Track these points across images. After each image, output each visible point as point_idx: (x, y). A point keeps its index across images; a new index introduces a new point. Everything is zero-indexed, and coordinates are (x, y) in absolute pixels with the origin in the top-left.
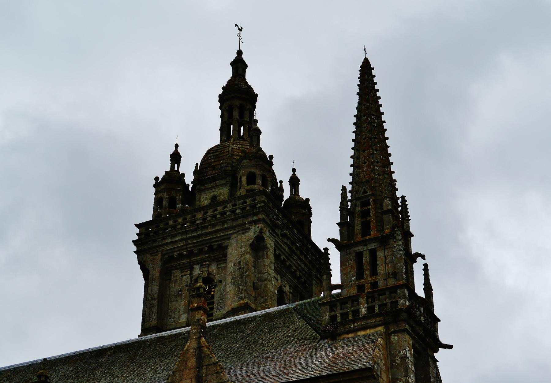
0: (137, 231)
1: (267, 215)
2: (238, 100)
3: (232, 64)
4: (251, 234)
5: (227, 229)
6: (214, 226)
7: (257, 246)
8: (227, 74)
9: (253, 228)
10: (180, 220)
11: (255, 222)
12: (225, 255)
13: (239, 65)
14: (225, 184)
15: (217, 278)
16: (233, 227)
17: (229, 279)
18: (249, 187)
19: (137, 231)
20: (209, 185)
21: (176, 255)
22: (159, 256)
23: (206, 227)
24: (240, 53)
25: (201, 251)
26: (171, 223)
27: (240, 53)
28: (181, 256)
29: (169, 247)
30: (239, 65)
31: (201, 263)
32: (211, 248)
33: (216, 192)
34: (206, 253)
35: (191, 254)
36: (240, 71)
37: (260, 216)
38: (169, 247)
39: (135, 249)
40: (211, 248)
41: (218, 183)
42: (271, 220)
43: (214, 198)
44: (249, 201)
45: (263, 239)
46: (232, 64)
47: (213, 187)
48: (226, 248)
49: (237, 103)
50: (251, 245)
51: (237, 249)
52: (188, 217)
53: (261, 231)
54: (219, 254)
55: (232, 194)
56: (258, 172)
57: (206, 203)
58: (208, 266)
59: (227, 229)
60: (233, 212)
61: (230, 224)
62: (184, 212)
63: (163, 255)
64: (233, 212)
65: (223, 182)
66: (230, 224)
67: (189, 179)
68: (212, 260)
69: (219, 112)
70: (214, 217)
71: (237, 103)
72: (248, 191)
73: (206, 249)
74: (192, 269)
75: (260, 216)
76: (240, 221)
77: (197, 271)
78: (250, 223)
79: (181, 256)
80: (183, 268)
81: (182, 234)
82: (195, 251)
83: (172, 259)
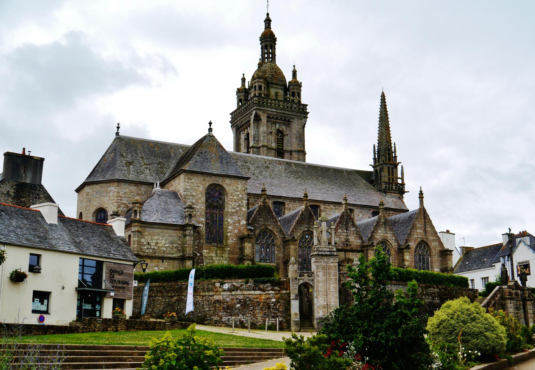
2: (268, 41)
13: (268, 21)
14: (282, 89)
20: (274, 86)
21: (271, 116)
22: (266, 115)
25: (281, 119)
28: (273, 118)
30: (268, 21)
31: (279, 123)
35: (277, 118)
40: (285, 119)
41: (278, 87)
48: (291, 122)
65: (280, 87)
68: (284, 124)
77: (277, 126)
79: (273, 118)
81: (277, 109)
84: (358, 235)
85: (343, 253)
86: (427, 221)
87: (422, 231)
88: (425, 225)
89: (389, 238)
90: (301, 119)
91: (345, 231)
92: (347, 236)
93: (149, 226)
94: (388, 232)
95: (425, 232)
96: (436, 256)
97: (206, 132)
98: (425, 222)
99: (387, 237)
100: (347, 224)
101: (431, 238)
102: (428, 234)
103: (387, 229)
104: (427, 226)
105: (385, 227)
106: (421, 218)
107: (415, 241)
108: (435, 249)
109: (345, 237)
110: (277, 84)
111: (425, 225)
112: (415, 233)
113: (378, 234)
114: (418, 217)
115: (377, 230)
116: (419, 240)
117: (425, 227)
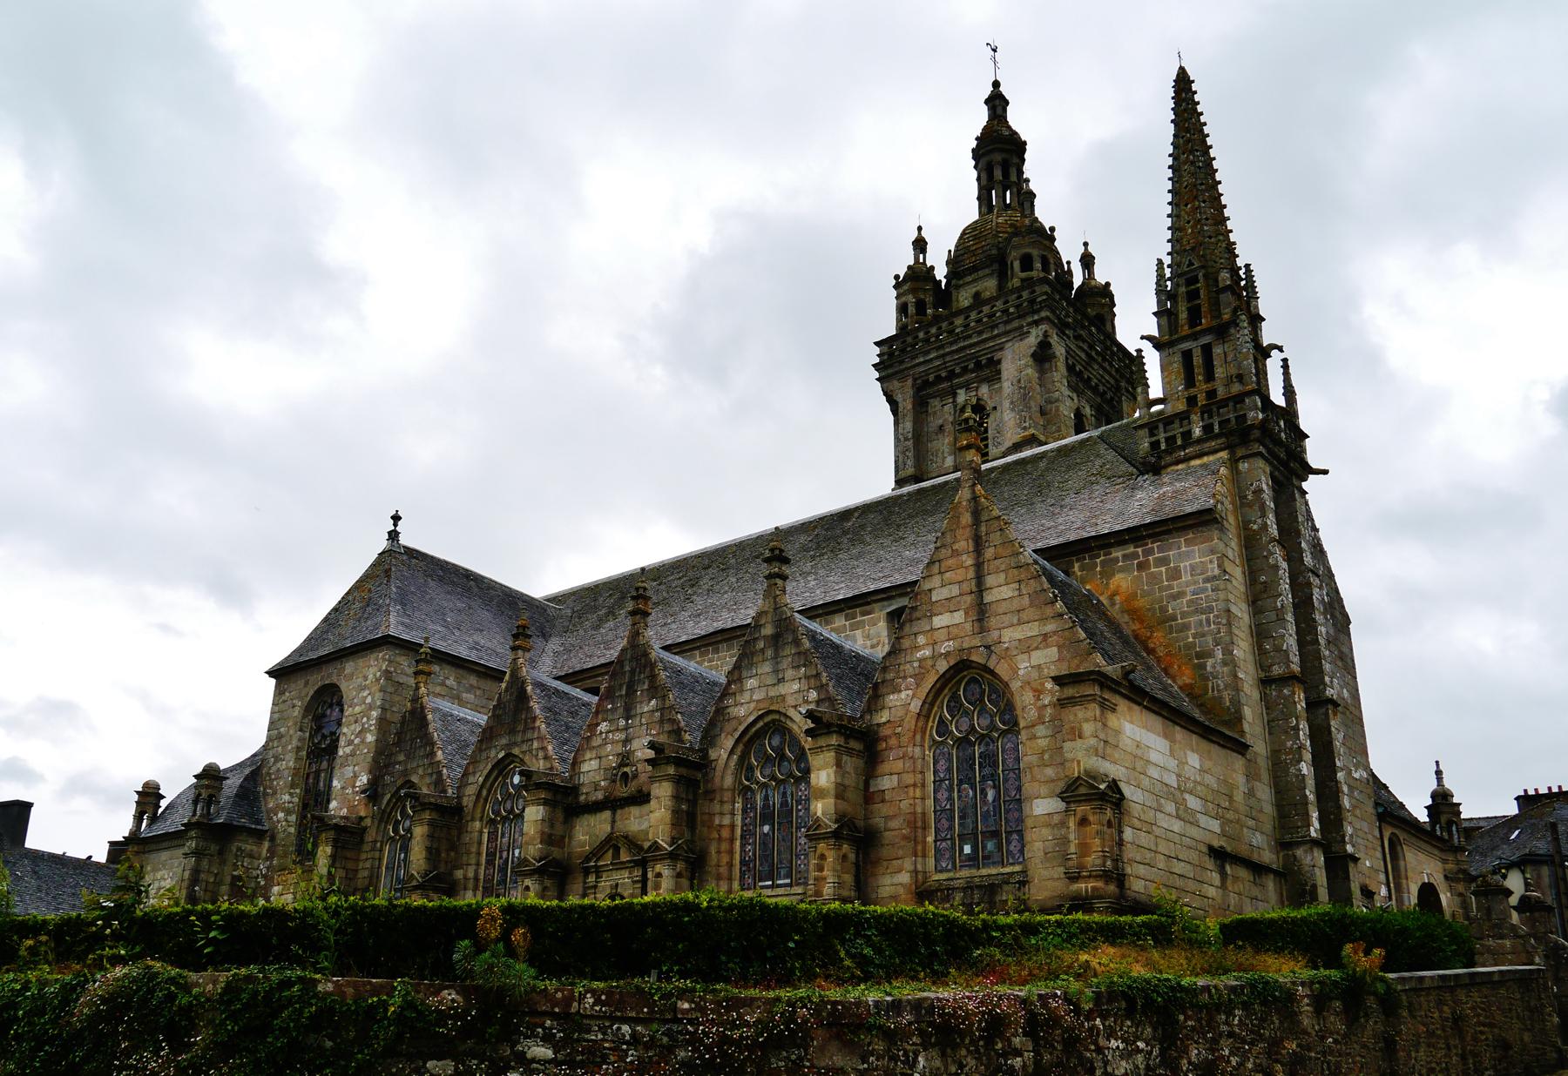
0: (877, 350)
1: (1053, 312)
2: (999, 153)
3: (987, 102)
4: (1033, 340)
5: (998, 336)
6: (980, 333)
7: (1042, 356)
8: (981, 117)
9: (1034, 331)
10: (933, 330)
11: (1036, 323)
12: (999, 372)
13: (997, 102)
14: (991, 274)
15: (990, 405)
16: (1006, 333)
17: (1006, 404)
18: (1024, 275)
19: (877, 350)
20: (969, 279)
22: (910, 382)
23: (970, 337)
24: (996, 84)
25: (965, 370)
26: (921, 335)
27: (996, 84)
28: (939, 379)
29: (922, 369)
30: (997, 102)
32: (978, 366)
33: (978, 287)
34: (972, 371)
35: (952, 375)
36: (999, 111)
37: (1043, 314)
38: (922, 369)
39: (877, 375)
40: (978, 366)
41: (981, 273)
42: (1059, 318)
43: (977, 295)
44: (1025, 294)
45: (1049, 345)
46: (987, 102)
47: (974, 281)
48: (999, 361)
49: (998, 157)
50: (1033, 355)
51: (1015, 361)
52: (944, 325)
53: (1046, 335)
54: (989, 370)
55: (1001, 287)
56: (1035, 252)
57: (966, 303)
58: (977, 389)
59: (998, 336)
60: (1005, 311)
61: (1002, 328)
62: (937, 319)
63: (915, 380)
64: (1005, 311)
65: (987, 271)
66: (1002, 328)
67: (941, 273)
68: (982, 381)
69: (975, 174)
70: (979, 321)
71: (998, 157)
72: (1023, 280)
73: (971, 366)
74: (955, 395)
75: (1043, 314)
76: (1015, 324)
77: (962, 397)
78: (1029, 324)
79: (939, 379)
80: (942, 395)
81: (938, 348)
82: (958, 370)
83: (926, 384)
84: (667, 727)
85: (607, 814)
86: (989, 553)
87: (958, 617)
88: (979, 578)
89: (791, 701)
90: (1024, 335)
91: (622, 723)
92: (627, 741)
93: (153, 847)
94: (790, 673)
95: (981, 612)
96: (1041, 730)
97: (382, 544)
98: (979, 566)
99: (783, 697)
100: (631, 691)
101: (1010, 636)
102: (993, 622)
103: (785, 663)
104: (990, 580)
105: (776, 657)
106: (956, 553)
107: (919, 677)
108: (1038, 693)
109: (619, 749)
110: (975, 269)
111: (979, 578)
112: (921, 640)
113: (746, 697)
114: (944, 553)
115: (740, 680)
116: (943, 666)
117: (980, 588)
